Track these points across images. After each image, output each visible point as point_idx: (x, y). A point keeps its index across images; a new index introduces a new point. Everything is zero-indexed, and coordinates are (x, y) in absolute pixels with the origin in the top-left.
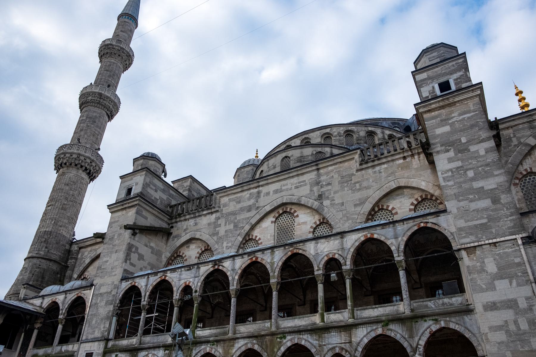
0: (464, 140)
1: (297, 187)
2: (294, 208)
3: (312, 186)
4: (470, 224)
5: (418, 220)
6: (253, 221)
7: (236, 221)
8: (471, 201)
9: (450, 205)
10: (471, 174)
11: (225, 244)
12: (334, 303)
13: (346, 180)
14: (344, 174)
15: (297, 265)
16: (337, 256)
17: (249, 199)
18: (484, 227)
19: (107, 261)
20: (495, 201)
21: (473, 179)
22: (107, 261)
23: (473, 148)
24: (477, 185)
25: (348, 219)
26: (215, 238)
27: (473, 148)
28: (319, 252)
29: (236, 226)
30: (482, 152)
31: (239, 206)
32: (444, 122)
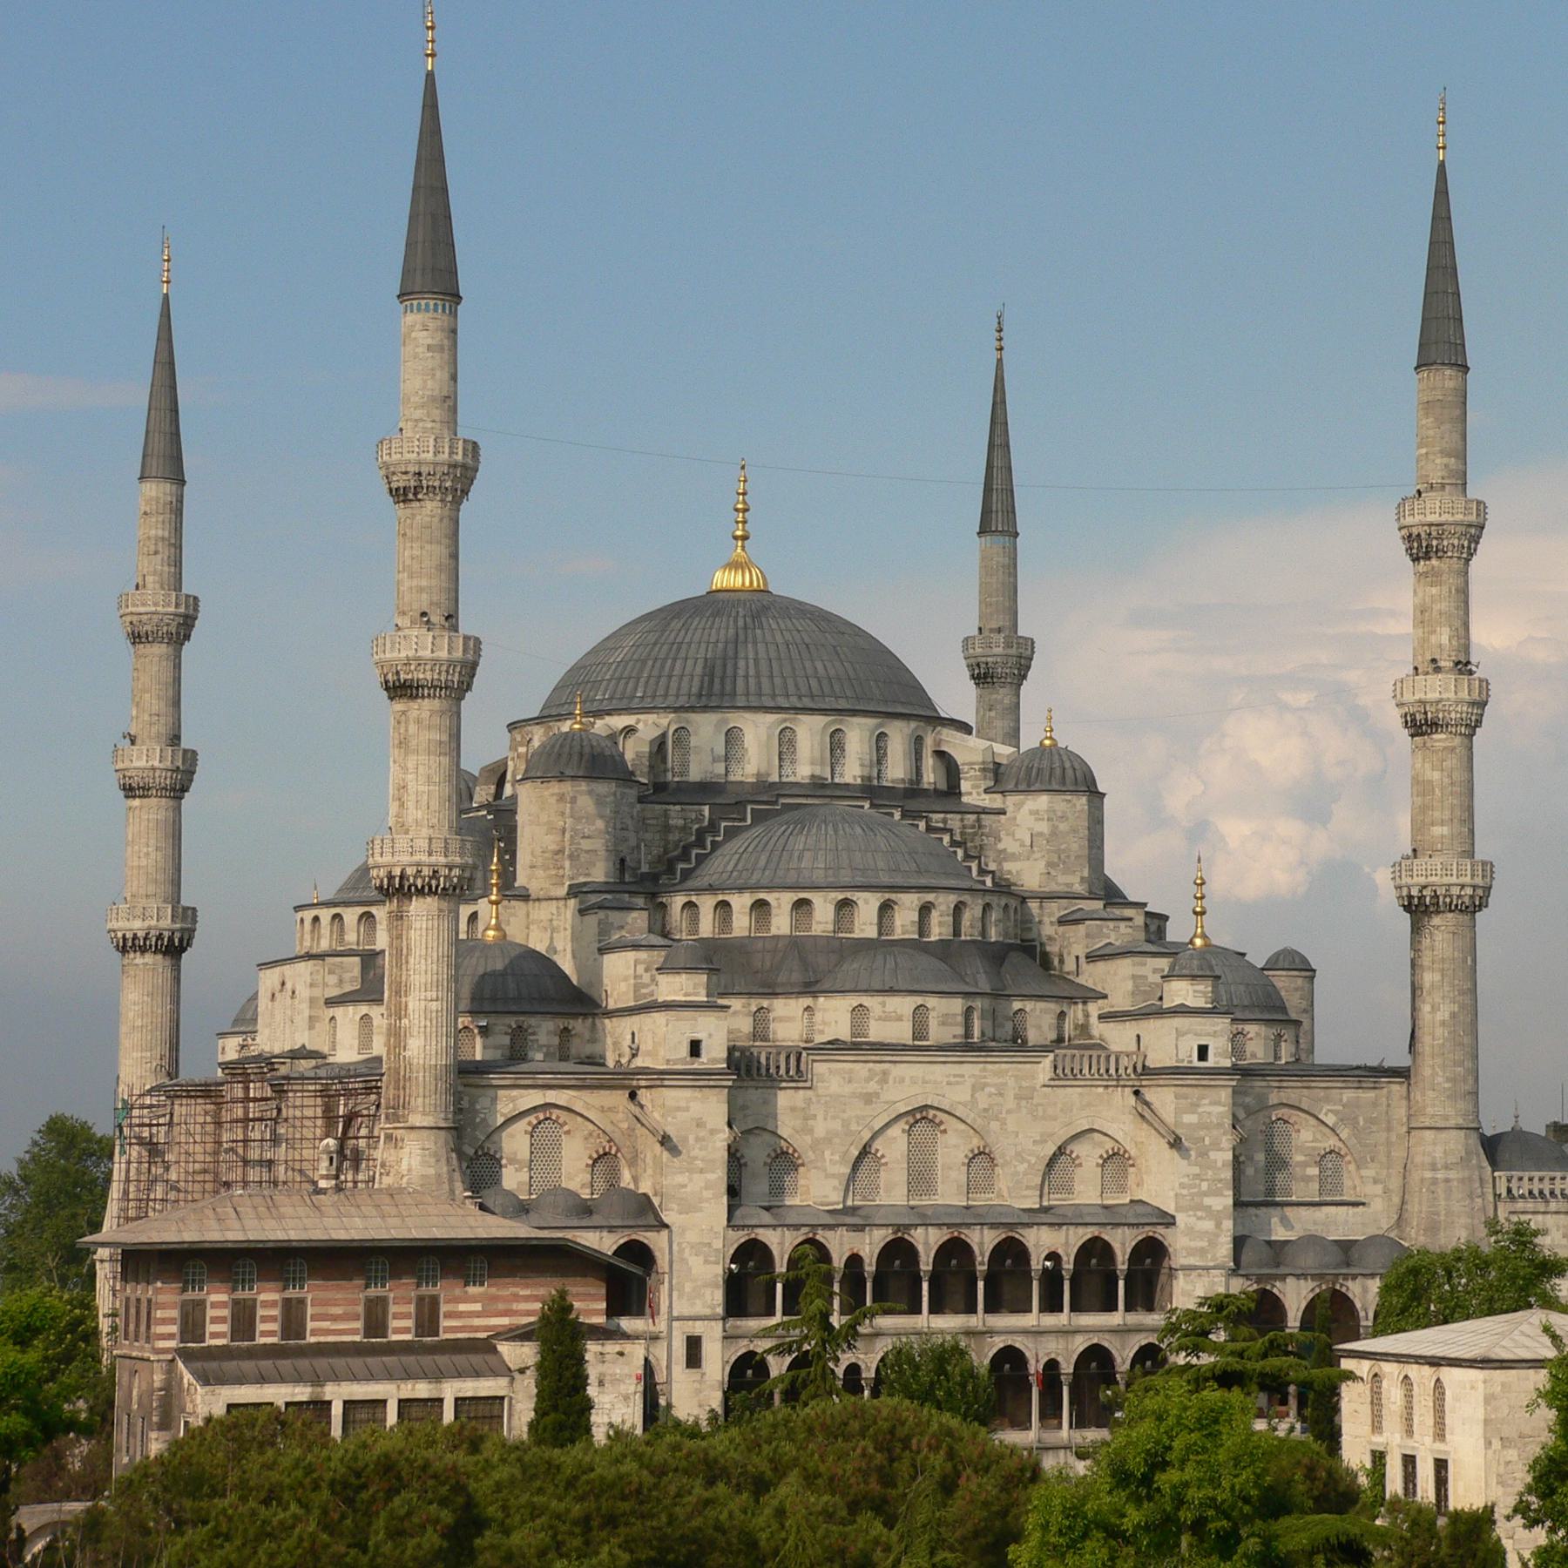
0: (1207, 1141)
1: (949, 1083)
2: (941, 1116)
3: (974, 1089)
4: (1193, 1244)
5: (1147, 1228)
6: (877, 1125)
7: (845, 1116)
8: (1199, 1218)
9: (1181, 1219)
10: (1205, 1186)
11: (827, 1154)
12: (1052, 1304)
13: (1024, 1096)
14: (1024, 1084)
15: (1011, 1252)
16: (1060, 1251)
17: (868, 1080)
18: (1202, 1252)
19: (685, 1186)
20: (1218, 1225)
21: (1205, 1194)
22: (685, 1186)
23: (1213, 1155)
24: (1207, 1201)
25: (1023, 1160)
26: (808, 1139)
27: (1213, 1155)
28: (1039, 1242)
29: (846, 1124)
30: (1219, 1164)
31: (848, 1089)
32: (1193, 1108)
